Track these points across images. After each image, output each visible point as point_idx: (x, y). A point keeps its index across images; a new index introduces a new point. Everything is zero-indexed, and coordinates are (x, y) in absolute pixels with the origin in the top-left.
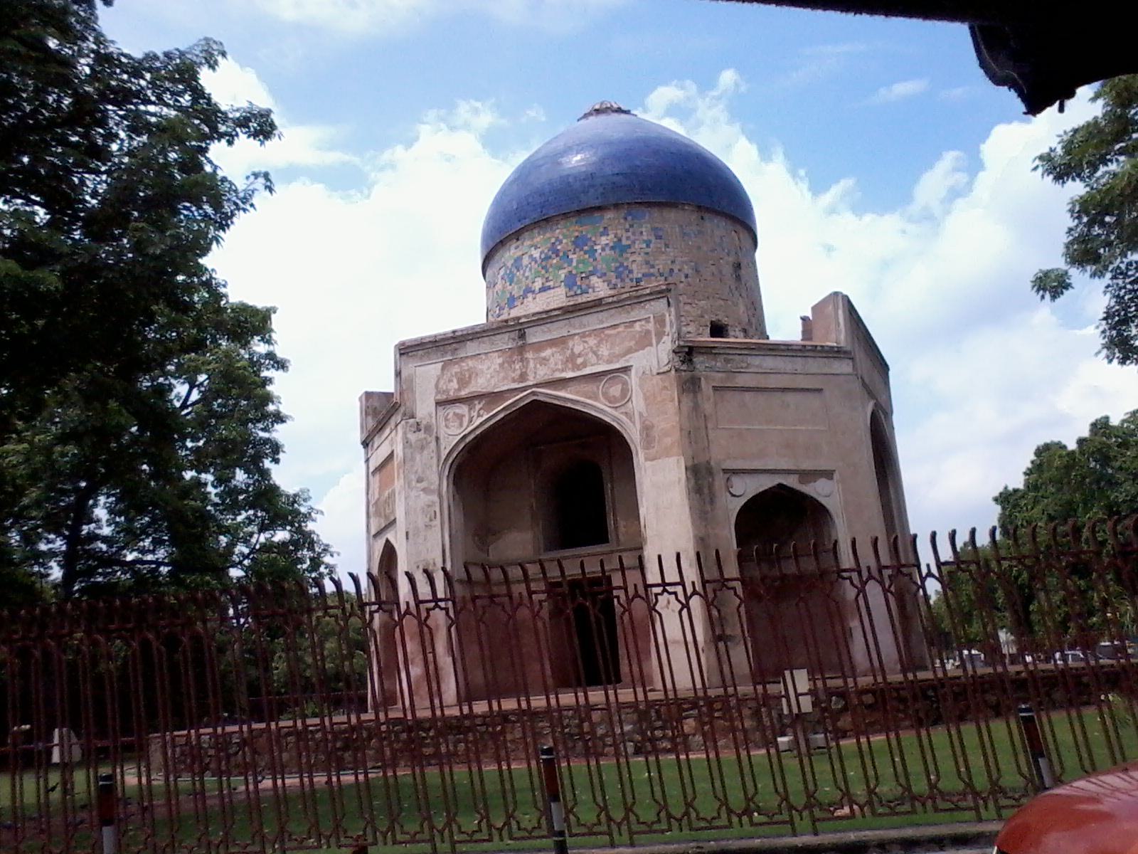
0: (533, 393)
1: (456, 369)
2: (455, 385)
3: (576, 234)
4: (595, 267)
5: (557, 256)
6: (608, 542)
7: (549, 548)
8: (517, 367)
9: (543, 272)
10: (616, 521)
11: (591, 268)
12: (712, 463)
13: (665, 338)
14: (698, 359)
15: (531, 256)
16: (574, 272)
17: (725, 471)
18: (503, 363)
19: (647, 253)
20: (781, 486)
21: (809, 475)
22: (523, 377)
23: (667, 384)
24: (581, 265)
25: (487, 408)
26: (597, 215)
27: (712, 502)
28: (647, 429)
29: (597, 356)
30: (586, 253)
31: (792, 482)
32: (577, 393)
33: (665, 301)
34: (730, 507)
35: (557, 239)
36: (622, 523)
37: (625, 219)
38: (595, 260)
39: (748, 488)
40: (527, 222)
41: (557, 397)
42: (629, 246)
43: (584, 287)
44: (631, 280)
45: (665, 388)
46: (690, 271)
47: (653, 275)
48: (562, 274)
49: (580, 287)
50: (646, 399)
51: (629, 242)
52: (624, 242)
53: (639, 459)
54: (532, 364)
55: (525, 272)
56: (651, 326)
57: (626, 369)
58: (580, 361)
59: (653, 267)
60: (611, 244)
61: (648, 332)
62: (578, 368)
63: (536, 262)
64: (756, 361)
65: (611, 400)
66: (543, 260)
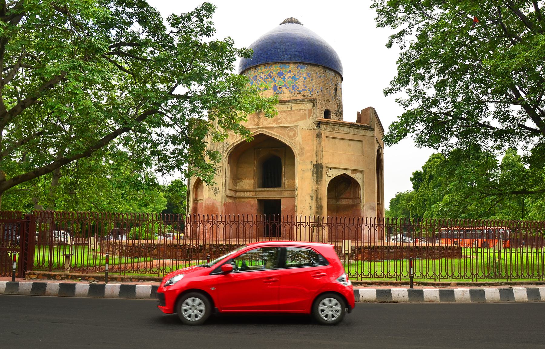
0: (261, 131)
3: (279, 71)
4: (285, 85)
5: (271, 78)
6: (280, 186)
7: (259, 187)
8: (256, 120)
9: (265, 83)
10: (285, 180)
11: (283, 85)
12: (323, 164)
13: (311, 117)
14: (323, 127)
15: (260, 76)
16: (277, 85)
17: (327, 167)
18: (251, 118)
19: (304, 82)
20: (344, 174)
21: (354, 171)
22: (258, 124)
23: (310, 134)
24: (279, 83)
26: (287, 65)
27: (321, 177)
28: (302, 149)
29: (286, 120)
30: (282, 78)
31: (348, 173)
32: (277, 133)
33: (312, 104)
34: (327, 180)
35: (271, 72)
36: (287, 181)
37: (298, 68)
38: (285, 82)
39: (334, 174)
41: (270, 133)
42: (298, 79)
43: (280, 91)
44: (298, 91)
45: (309, 135)
46: (319, 90)
47: (306, 90)
48: (272, 85)
49: (278, 91)
50: (302, 138)
51: (298, 77)
52: (296, 77)
53: (297, 160)
54: (261, 120)
55: (257, 82)
56: (307, 112)
57: (296, 127)
58: (279, 121)
59: (306, 87)
60: (292, 77)
61: (305, 114)
62: (279, 123)
63: (262, 79)
64: (342, 129)
65: (290, 137)
66: (265, 79)
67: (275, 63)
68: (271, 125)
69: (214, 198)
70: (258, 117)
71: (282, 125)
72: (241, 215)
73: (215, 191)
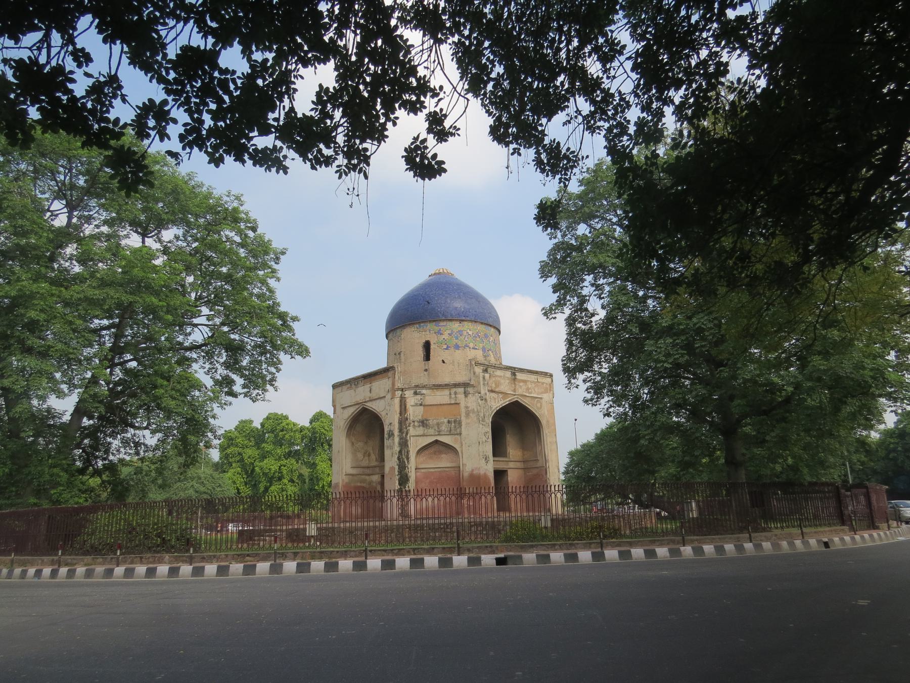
2: (494, 385)
22: (514, 391)
25: (503, 398)
28: (548, 421)
40: (468, 319)
57: (541, 398)
67: (482, 323)
69: (486, 467)
70: (515, 384)
71: (532, 395)
72: (420, 490)
73: (486, 459)
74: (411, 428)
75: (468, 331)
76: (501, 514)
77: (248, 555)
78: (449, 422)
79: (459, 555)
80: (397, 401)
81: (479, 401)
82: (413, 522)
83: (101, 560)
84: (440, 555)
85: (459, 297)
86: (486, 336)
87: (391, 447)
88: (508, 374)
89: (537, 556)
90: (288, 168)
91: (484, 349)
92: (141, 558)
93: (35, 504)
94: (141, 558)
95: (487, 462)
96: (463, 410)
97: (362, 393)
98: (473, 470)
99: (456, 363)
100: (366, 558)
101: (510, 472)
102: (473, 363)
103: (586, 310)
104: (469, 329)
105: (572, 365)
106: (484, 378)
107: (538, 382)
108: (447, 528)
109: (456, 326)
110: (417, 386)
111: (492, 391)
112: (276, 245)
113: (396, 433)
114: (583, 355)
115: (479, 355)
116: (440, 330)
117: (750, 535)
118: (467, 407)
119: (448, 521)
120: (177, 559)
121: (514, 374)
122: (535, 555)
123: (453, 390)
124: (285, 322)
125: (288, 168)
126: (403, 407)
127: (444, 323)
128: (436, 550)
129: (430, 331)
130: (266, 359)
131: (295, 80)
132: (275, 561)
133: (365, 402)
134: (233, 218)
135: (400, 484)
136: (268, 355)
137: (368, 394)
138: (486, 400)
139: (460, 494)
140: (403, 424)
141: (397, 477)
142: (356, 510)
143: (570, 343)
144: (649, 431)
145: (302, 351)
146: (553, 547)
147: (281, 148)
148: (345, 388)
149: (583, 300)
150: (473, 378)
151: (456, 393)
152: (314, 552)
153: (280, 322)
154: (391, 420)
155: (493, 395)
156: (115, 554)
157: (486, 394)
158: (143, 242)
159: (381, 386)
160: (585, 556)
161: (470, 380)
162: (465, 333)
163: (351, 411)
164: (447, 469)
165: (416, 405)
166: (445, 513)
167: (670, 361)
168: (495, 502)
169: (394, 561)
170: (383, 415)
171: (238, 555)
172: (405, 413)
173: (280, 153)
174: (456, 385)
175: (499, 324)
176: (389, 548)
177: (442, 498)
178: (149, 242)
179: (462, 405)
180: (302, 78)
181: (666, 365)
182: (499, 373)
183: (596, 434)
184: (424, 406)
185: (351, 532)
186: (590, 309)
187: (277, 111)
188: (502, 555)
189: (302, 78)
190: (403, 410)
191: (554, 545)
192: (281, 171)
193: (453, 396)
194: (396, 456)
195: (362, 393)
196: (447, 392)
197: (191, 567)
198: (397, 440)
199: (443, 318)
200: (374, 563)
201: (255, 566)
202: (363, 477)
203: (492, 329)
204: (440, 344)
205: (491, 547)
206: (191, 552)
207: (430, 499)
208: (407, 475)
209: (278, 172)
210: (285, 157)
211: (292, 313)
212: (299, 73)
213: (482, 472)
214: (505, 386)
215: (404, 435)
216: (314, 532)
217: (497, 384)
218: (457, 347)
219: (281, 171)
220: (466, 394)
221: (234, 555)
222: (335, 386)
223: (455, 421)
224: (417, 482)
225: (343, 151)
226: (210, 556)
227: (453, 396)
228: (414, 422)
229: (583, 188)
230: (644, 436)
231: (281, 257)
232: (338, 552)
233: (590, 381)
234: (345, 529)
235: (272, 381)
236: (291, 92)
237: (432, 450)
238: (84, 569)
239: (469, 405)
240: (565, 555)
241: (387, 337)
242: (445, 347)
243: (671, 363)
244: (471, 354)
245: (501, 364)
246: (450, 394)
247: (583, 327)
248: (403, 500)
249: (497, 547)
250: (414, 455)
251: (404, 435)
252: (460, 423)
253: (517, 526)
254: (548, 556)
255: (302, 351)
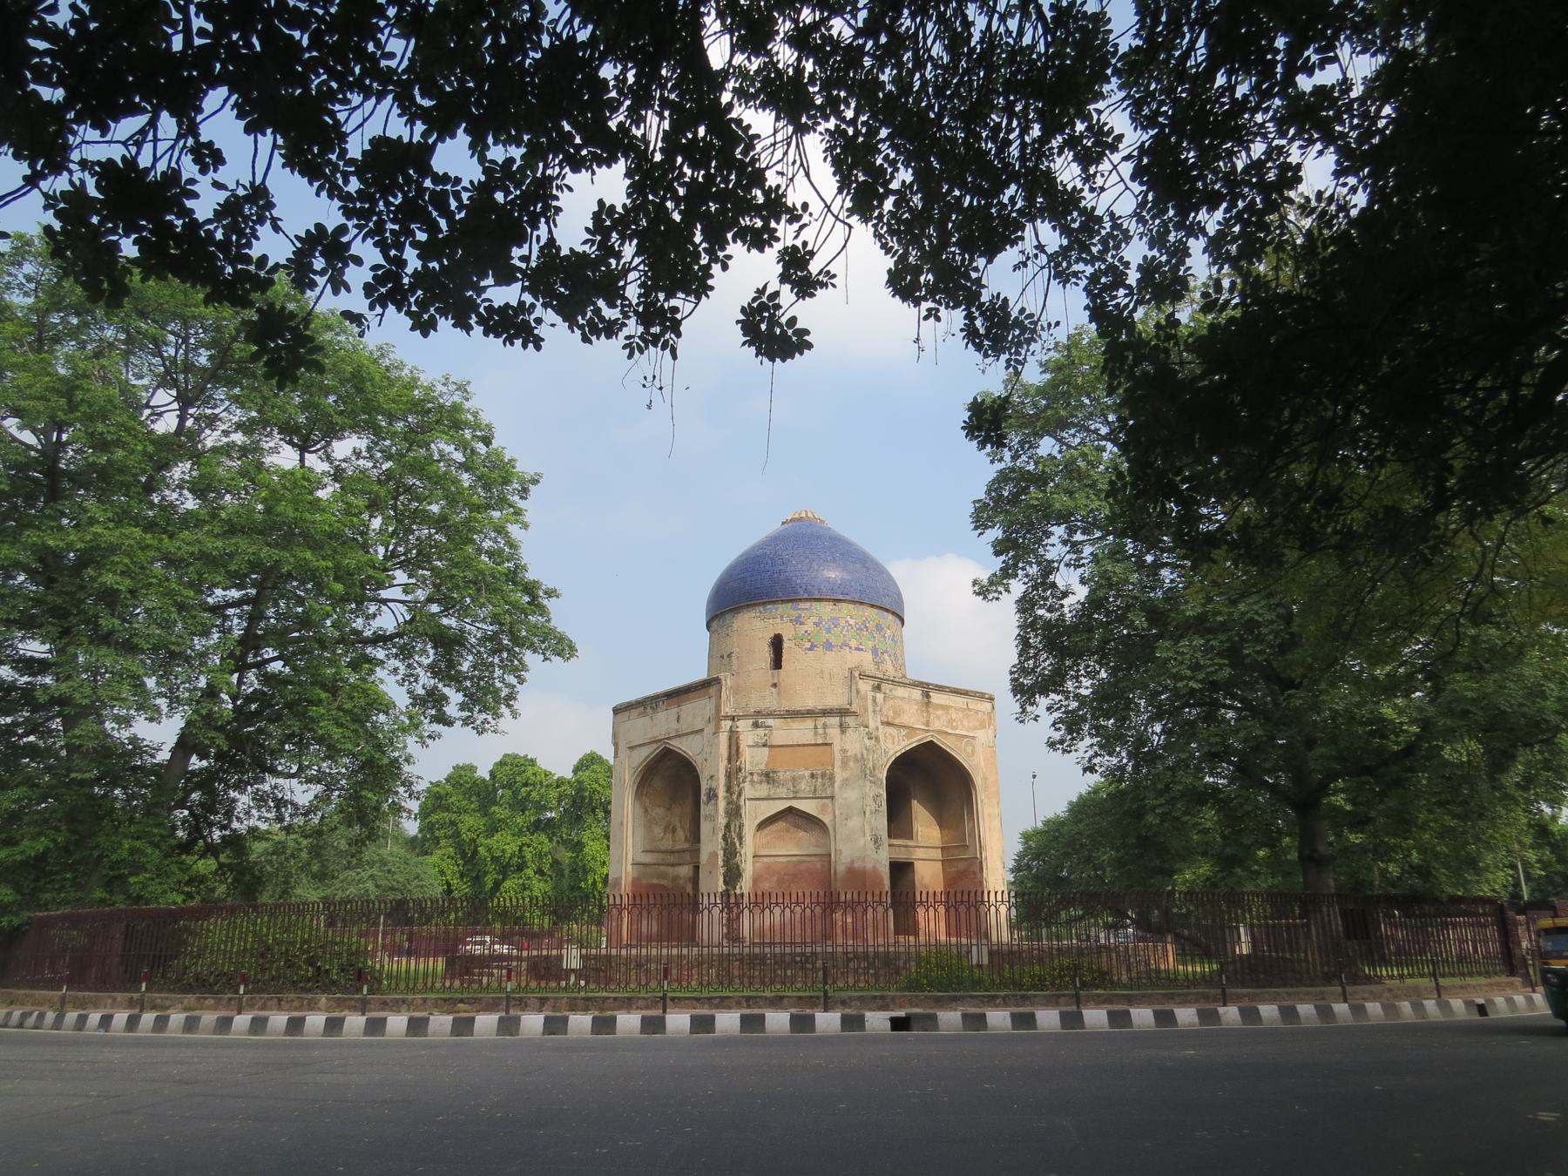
1: (891, 703)
2: (891, 714)
22: (927, 724)
25: (908, 736)
28: (985, 778)
40: (848, 598)
48: (870, 644)
57: (974, 738)
67: (872, 606)
68: (944, 729)
69: (875, 856)
71: (957, 732)
72: (759, 893)
73: (876, 842)
74: (747, 785)
75: (849, 619)
76: (901, 938)
77: (461, 1001)
78: (812, 776)
79: (826, 1011)
80: (723, 738)
81: (866, 740)
82: (747, 950)
83: (212, 1002)
84: (794, 1011)
85: (834, 560)
86: (879, 628)
87: (713, 818)
88: (917, 694)
89: (964, 1016)
90: (543, 340)
91: (875, 651)
92: (280, 1000)
93: (102, 901)
94: (280, 1000)
95: (878, 848)
96: (838, 756)
97: (663, 723)
98: (852, 862)
99: (826, 675)
100: (665, 1011)
101: (917, 864)
102: (856, 674)
103: (1054, 585)
104: (849, 614)
105: (1027, 681)
106: (874, 700)
107: (970, 710)
108: (807, 962)
109: (826, 609)
110: (758, 713)
111: (888, 724)
112: (524, 467)
113: (721, 793)
114: (1047, 663)
115: (866, 660)
116: (800, 616)
117: (1224, 990)
118: (844, 751)
119: (809, 950)
120: (340, 1004)
121: (928, 696)
122: (959, 1014)
123: (823, 720)
124: (534, 597)
125: (543, 340)
126: (734, 748)
127: (807, 605)
128: (785, 1001)
129: (782, 617)
130: (502, 661)
131: (559, 194)
132: (507, 1012)
133: (669, 738)
134: (452, 420)
135: (726, 883)
136: (505, 655)
137: (674, 725)
138: (877, 738)
139: (830, 902)
140: (733, 779)
141: (722, 871)
142: (649, 926)
143: (1024, 643)
144: (1162, 801)
145: (562, 648)
146: (992, 1001)
147: (533, 306)
148: (635, 713)
149: (1048, 568)
150: (855, 701)
151: (825, 726)
152: (575, 998)
153: (527, 599)
154: (713, 772)
155: (889, 730)
156: (237, 992)
157: (877, 728)
158: (302, 460)
159: (696, 711)
160: (1048, 1018)
161: (851, 704)
162: (843, 623)
163: (644, 754)
164: (807, 859)
165: (756, 745)
166: (803, 935)
167: (1201, 676)
168: (891, 918)
169: (713, 1017)
170: (698, 762)
171: (445, 1000)
172: (738, 758)
173: (530, 314)
174: (826, 713)
175: (902, 609)
176: (705, 994)
177: (798, 909)
178: (312, 460)
179: (837, 748)
180: (570, 189)
181: (1192, 684)
182: (900, 692)
183: (1070, 803)
184: (771, 746)
185: (639, 966)
186: (1061, 583)
187: (526, 246)
188: (901, 1013)
189: (570, 189)
190: (733, 753)
191: (995, 997)
192: (531, 345)
193: (820, 731)
194: (721, 835)
195: (663, 723)
196: (809, 723)
197: (364, 1018)
198: (722, 805)
199: (806, 596)
200: (629, 1022)
201: (472, 1020)
202: (662, 868)
203: (890, 617)
204: (798, 640)
205: (882, 997)
206: (365, 992)
207: (777, 911)
208: (738, 867)
209: (525, 346)
210: (539, 321)
211: (548, 582)
212: (565, 182)
213: (869, 865)
214: (911, 715)
215: (735, 797)
216: (575, 964)
217: (897, 713)
218: (828, 646)
219: (531, 345)
220: (843, 728)
221: (436, 999)
222: (617, 711)
223: (823, 776)
224: (755, 881)
225: (635, 312)
226: (397, 1001)
227: (820, 731)
228: (752, 774)
229: (1048, 376)
230: (1154, 808)
231: (532, 487)
232: (615, 999)
233: (1059, 709)
234: (629, 959)
235: (511, 697)
236: (550, 212)
237: (781, 825)
238: (125, 1015)
239: (847, 747)
240: (1013, 1016)
241: (708, 626)
242: (808, 645)
243: (1201, 682)
244: (853, 659)
245: (904, 676)
246: (816, 728)
247: (1048, 615)
248: (730, 910)
249: (893, 999)
250: (752, 833)
251: (735, 797)
252: (832, 778)
253: (929, 963)
254: (984, 1016)
255: (562, 648)
